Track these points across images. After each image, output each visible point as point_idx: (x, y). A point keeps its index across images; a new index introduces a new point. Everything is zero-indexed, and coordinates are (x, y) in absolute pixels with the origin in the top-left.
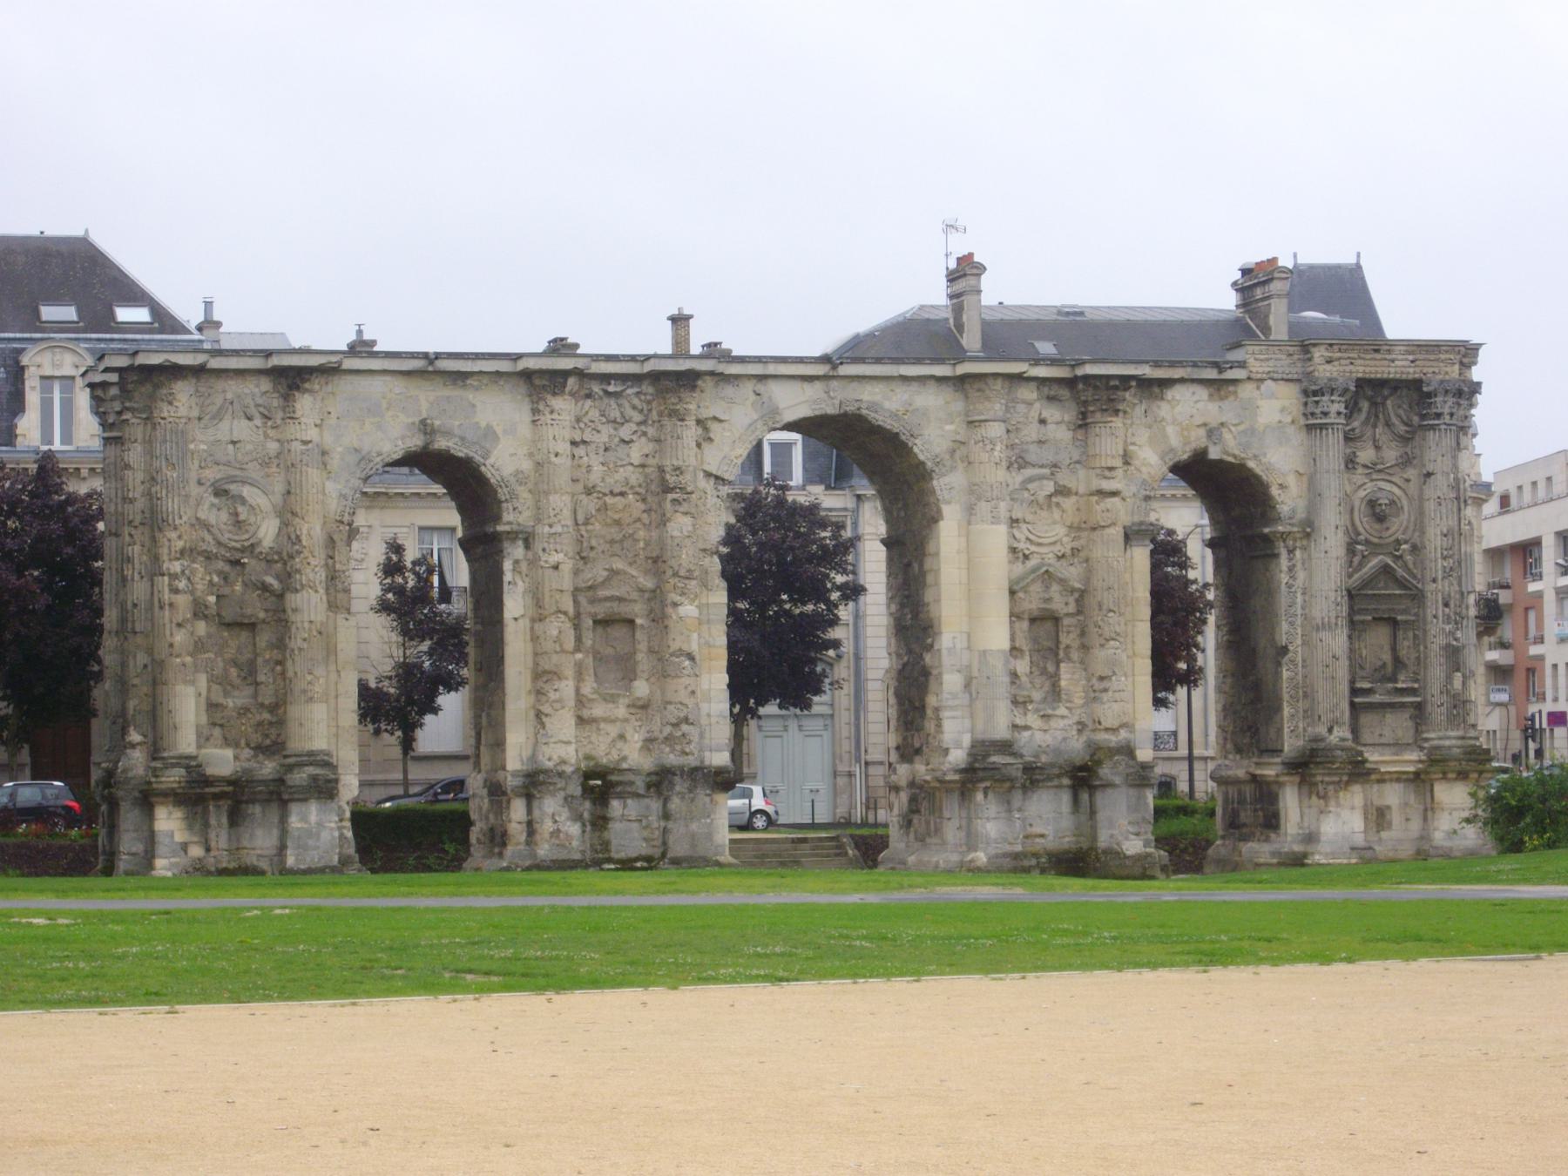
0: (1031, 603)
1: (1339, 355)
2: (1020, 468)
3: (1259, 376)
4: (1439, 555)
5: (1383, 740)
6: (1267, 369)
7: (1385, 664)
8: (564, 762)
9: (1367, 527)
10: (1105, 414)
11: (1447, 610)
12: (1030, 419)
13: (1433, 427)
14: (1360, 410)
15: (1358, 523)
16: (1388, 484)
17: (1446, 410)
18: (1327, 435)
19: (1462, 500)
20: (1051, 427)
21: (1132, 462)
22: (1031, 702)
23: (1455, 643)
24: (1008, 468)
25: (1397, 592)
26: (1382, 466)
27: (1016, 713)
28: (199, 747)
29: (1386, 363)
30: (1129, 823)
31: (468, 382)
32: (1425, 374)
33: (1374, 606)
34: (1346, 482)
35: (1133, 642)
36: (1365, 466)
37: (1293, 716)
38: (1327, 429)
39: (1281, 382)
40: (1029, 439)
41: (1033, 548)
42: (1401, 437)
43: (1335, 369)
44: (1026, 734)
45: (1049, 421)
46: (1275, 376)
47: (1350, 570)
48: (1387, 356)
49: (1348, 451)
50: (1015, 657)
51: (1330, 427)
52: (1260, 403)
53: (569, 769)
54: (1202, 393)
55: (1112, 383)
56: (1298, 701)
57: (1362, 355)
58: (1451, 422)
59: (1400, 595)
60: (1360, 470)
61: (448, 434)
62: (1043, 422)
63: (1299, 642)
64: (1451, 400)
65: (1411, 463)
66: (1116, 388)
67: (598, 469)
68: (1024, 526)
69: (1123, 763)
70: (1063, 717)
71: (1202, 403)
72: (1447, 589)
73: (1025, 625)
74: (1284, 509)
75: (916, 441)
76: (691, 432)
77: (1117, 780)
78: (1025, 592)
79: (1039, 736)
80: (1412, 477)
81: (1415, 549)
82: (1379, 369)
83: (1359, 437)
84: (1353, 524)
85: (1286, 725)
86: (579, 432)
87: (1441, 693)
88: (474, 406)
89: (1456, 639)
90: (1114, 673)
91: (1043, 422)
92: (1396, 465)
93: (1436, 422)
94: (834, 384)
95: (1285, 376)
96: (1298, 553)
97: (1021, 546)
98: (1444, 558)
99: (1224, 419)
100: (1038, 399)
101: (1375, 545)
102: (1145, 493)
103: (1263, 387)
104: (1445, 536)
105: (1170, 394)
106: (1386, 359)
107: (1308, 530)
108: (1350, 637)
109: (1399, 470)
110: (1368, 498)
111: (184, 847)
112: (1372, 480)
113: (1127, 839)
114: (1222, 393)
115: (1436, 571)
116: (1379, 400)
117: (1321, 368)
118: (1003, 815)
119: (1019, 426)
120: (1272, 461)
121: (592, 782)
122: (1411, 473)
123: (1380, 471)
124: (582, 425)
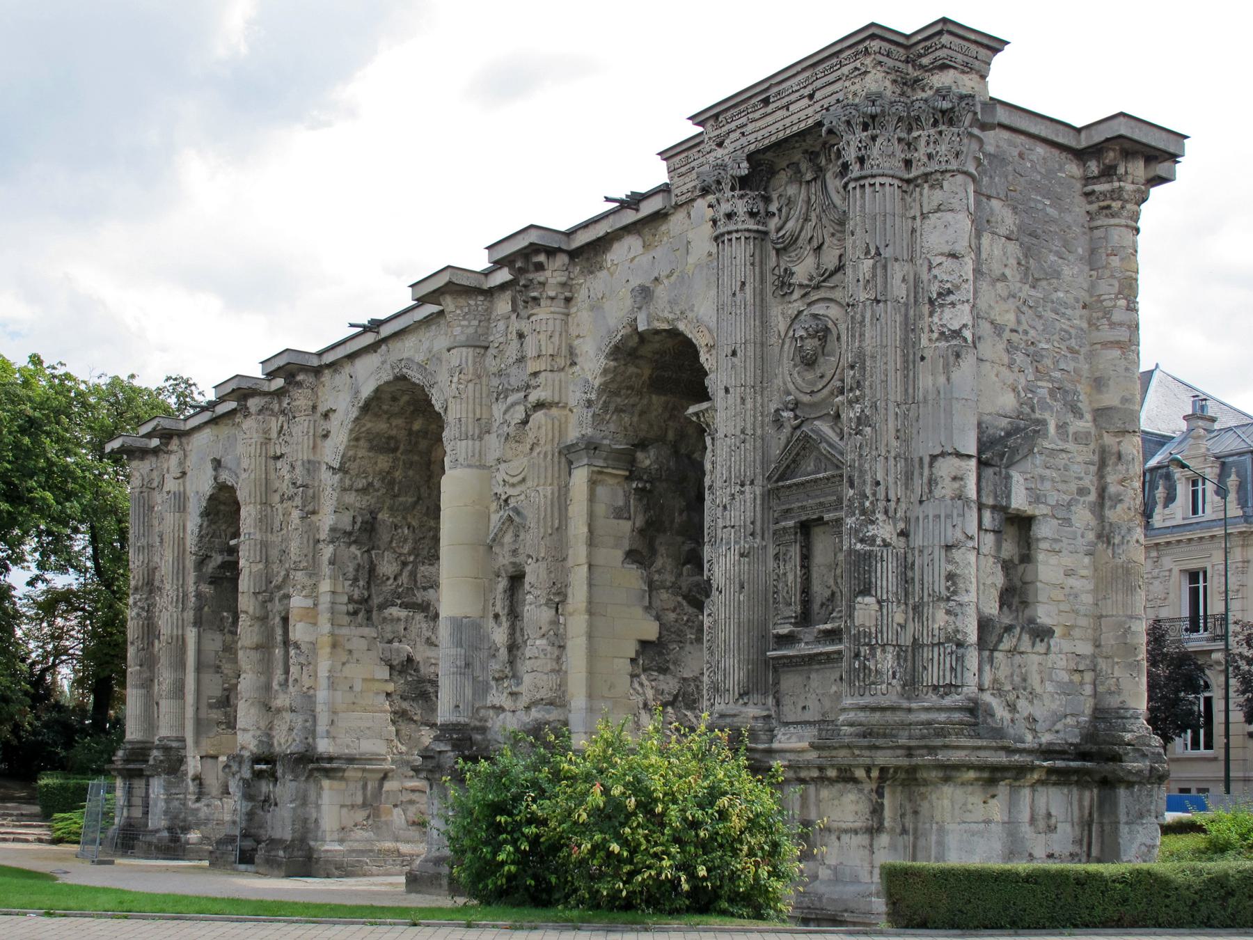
2: (506, 397)
9: (799, 381)
21: (576, 360)
25: (821, 475)
34: (780, 318)
36: (801, 286)
40: (511, 361)
41: (511, 491)
50: (500, 625)
52: (690, 236)
59: (828, 479)
60: (796, 295)
66: (522, 271)
68: (503, 466)
75: (433, 391)
76: (301, 427)
97: (500, 490)
101: (812, 405)
104: (852, 367)
123: (817, 287)
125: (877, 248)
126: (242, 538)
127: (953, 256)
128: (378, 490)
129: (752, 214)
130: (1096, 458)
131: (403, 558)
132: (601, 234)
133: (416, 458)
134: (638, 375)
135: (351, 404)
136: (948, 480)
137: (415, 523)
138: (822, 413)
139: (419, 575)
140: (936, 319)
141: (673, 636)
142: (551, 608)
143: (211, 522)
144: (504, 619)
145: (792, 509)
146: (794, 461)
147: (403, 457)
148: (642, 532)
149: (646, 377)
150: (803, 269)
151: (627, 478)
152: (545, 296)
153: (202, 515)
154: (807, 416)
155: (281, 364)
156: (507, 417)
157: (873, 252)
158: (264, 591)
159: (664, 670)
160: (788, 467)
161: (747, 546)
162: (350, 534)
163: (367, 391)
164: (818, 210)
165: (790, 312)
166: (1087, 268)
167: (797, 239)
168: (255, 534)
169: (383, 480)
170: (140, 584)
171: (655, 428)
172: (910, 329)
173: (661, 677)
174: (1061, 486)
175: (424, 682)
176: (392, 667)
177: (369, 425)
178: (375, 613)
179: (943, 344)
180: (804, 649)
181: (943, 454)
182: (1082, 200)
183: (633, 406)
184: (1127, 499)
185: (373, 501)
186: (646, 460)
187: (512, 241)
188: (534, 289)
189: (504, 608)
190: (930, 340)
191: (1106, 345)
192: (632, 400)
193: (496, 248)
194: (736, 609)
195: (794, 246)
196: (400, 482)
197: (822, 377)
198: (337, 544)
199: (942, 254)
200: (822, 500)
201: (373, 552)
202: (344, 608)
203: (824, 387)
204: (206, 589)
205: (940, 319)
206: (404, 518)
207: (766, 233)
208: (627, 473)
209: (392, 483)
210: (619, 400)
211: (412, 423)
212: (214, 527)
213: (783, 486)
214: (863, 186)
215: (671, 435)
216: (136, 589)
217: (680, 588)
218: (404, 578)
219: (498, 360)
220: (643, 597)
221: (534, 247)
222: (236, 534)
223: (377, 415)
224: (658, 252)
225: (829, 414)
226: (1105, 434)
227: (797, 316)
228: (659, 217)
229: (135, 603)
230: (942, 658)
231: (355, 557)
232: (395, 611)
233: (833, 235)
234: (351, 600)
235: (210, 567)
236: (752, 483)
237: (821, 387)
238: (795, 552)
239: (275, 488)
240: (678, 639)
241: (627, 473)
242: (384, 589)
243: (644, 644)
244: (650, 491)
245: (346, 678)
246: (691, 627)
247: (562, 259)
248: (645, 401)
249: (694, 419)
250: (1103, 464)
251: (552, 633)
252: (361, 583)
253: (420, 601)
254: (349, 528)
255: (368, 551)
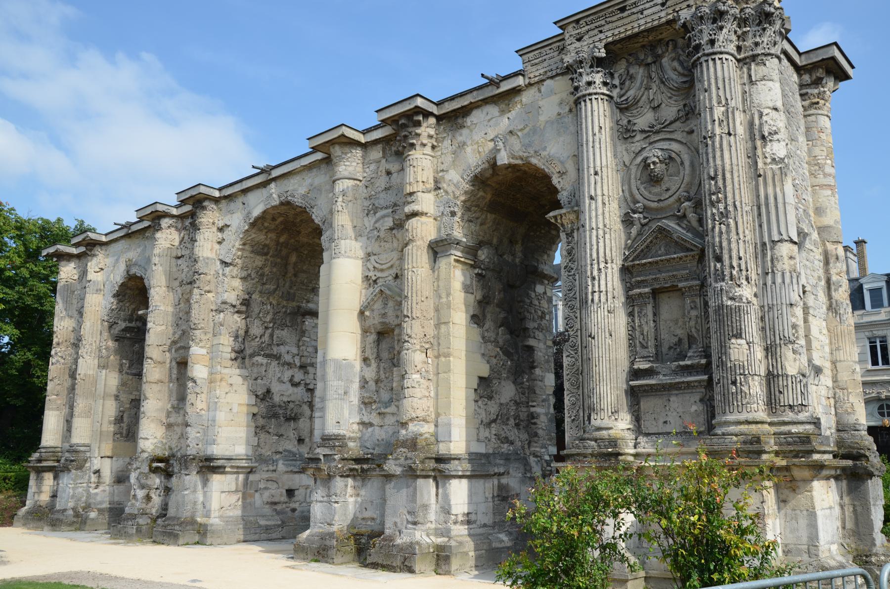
0: (375, 320)
1: (587, 28)
2: (375, 213)
3: (536, 79)
4: (708, 201)
5: (667, 429)
6: (542, 71)
7: (680, 340)
8: (143, 451)
9: (646, 193)
10: (406, 150)
11: (718, 265)
12: (379, 173)
13: (694, 65)
14: (632, 78)
15: (635, 192)
16: (667, 143)
17: (705, 38)
18: (581, 109)
19: (757, 137)
20: (395, 175)
22: (375, 402)
23: (729, 303)
24: (367, 215)
25: (675, 256)
26: (659, 126)
27: (364, 412)
28: (63, 442)
29: (634, 17)
30: (409, 513)
31: (147, 235)
32: (677, 12)
33: (651, 277)
34: (625, 153)
35: (439, 344)
36: (643, 131)
37: (573, 404)
38: (580, 103)
39: (557, 78)
40: (380, 189)
41: (379, 274)
42: (678, 89)
43: (585, 43)
44: (370, 430)
45: (393, 171)
46: (549, 74)
47: (629, 241)
48: (635, 10)
49: (625, 122)
50: (369, 365)
51: (582, 100)
52: (541, 103)
53: (145, 455)
54: (492, 110)
55: (400, 123)
56: (578, 388)
57: (608, 20)
58: (711, 51)
59: (681, 259)
60: (639, 137)
61: (135, 264)
62: (389, 173)
63: (578, 326)
64: (706, 28)
65: (693, 112)
66: (404, 126)
67: (186, 270)
68: (372, 258)
69: (404, 455)
70: (393, 414)
71: (494, 120)
72: (717, 239)
73: (372, 337)
74: (563, 196)
75: (314, 210)
77: (398, 471)
78: (373, 310)
79: (379, 434)
80: (695, 128)
81: (698, 205)
82: (629, 27)
83: (632, 105)
84: (632, 195)
85: (567, 415)
86: (180, 250)
87: (718, 366)
88: (146, 247)
89: (732, 299)
90: (407, 373)
91: (389, 173)
92: (675, 121)
93: (697, 56)
94: (273, 185)
95: (558, 71)
96: (575, 235)
97: (371, 274)
98: (712, 204)
99: (511, 128)
100: (384, 157)
101: (657, 210)
102: (448, 210)
103: (543, 89)
104: (713, 179)
105: (469, 120)
106: (634, 13)
107: (576, 208)
108: (631, 314)
109: (680, 125)
110: (643, 164)
111: (34, 493)
112: (651, 144)
113: (406, 528)
114: (511, 106)
115: (707, 221)
116: (649, 60)
117: (571, 48)
118: (325, 499)
119: (372, 181)
120: (552, 152)
121: (155, 465)
122: (692, 124)
123: (658, 132)
124: (182, 246)
125: (727, 99)
126: (150, 309)
127: (776, 109)
128: (253, 279)
129: (605, 84)
130: (821, 258)
131: (266, 324)
132: (466, 103)
133: (279, 260)
134: (483, 198)
135: (243, 221)
136: (786, 259)
137: (274, 302)
138: (668, 215)
139: (275, 336)
140: (768, 149)
141: (496, 374)
142: (422, 352)
143: (120, 301)
144: (373, 361)
145: (645, 280)
146: (647, 247)
147: (271, 259)
148: (480, 302)
149: (487, 200)
150: (645, 119)
151: (471, 266)
152: (419, 143)
153: (114, 296)
154: (653, 217)
155: (194, 193)
156: (377, 225)
157: (724, 102)
158: (165, 345)
159: (490, 398)
160: (642, 251)
161: (612, 306)
162: (234, 306)
163: (257, 212)
164: (657, 82)
165: (633, 149)
166: (805, 140)
167: (638, 101)
168: (160, 306)
169: (257, 273)
170: (61, 341)
171: (488, 235)
172: (752, 157)
173: (489, 402)
174: (813, 273)
175: (276, 407)
176: (257, 396)
177: (254, 236)
178: (247, 360)
179: (774, 167)
180: (662, 380)
181: (781, 241)
182: (798, 97)
183: (477, 218)
184: (844, 285)
185: (250, 286)
186: (483, 255)
187: (400, 105)
188: (413, 138)
189: (372, 354)
190: (765, 164)
191: (821, 186)
192: (478, 215)
193: (385, 111)
194: (607, 350)
195: (636, 107)
196: (268, 275)
197: (668, 190)
198: (226, 313)
199: (769, 108)
200: (674, 273)
201: (248, 319)
202: (229, 356)
203: (670, 197)
204: (110, 343)
205: (772, 150)
206: (268, 298)
207: (611, 97)
208: (473, 263)
209: (262, 275)
210: (470, 213)
211: (280, 237)
212: (121, 304)
213: (638, 264)
214: (714, 60)
215: (495, 241)
216: (58, 344)
217: (498, 342)
218: (266, 338)
219: (369, 189)
220: (481, 347)
221: (415, 110)
222: (147, 306)
223: (260, 230)
224: (513, 114)
225: (674, 215)
226: (827, 243)
227: (640, 151)
228: (516, 91)
229: (56, 354)
230: (794, 385)
231: (237, 322)
232: (259, 359)
233: (670, 98)
234: (233, 350)
235: (117, 330)
236: (612, 262)
237: (667, 197)
238: (649, 310)
239: (176, 277)
240: (498, 377)
241: (473, 263)
242: (253, 344)
243: (481, 379)
244: (484, 277)
245: (228, 403)
246: (504, 369)
247: (432, 120)
248: (483, 217)
249: (553, 221)
250: (827, 262)
251: (423, 370)
252: (240, 339)
253: (275, 353)
254: (234, 303)
255: (245, 318)
